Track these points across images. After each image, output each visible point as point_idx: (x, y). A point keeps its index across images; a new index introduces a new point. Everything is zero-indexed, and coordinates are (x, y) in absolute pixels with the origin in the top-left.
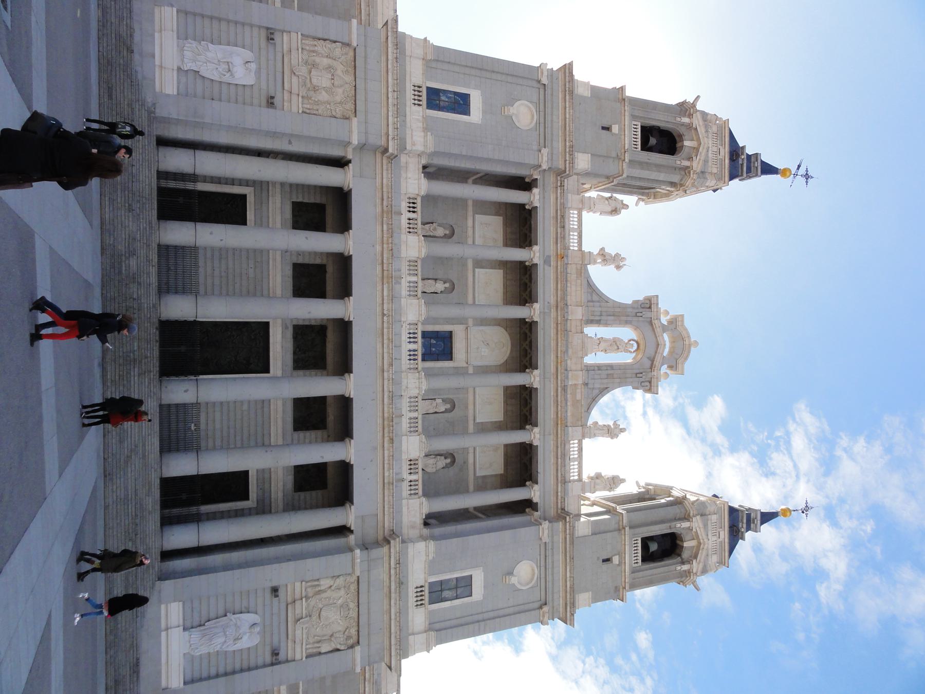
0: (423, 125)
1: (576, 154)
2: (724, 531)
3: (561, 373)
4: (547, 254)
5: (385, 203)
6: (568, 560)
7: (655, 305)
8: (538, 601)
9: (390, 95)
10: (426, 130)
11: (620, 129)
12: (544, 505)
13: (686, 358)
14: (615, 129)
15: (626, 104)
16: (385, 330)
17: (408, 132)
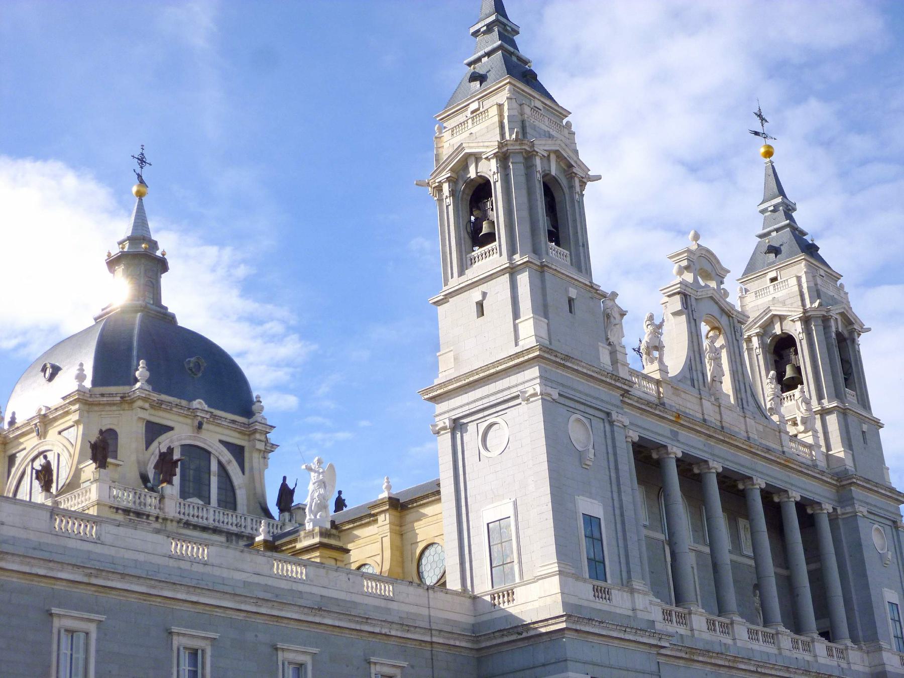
0: (624, 591)
1: (602, 365)
2: (819, 268)
3: (758, 450)
4: (669, 435)
5: (683, 655)
6: (875, 489)
7: (687, 289)
8: (892, 529)
9: (627, 637)
10: (632, 591)
11: (576, 287)
12: (832, 500)
13: (718, 262)
14: (573, 293)
15: (550, 265)
16: (767, 671)
17: (640, 615)
